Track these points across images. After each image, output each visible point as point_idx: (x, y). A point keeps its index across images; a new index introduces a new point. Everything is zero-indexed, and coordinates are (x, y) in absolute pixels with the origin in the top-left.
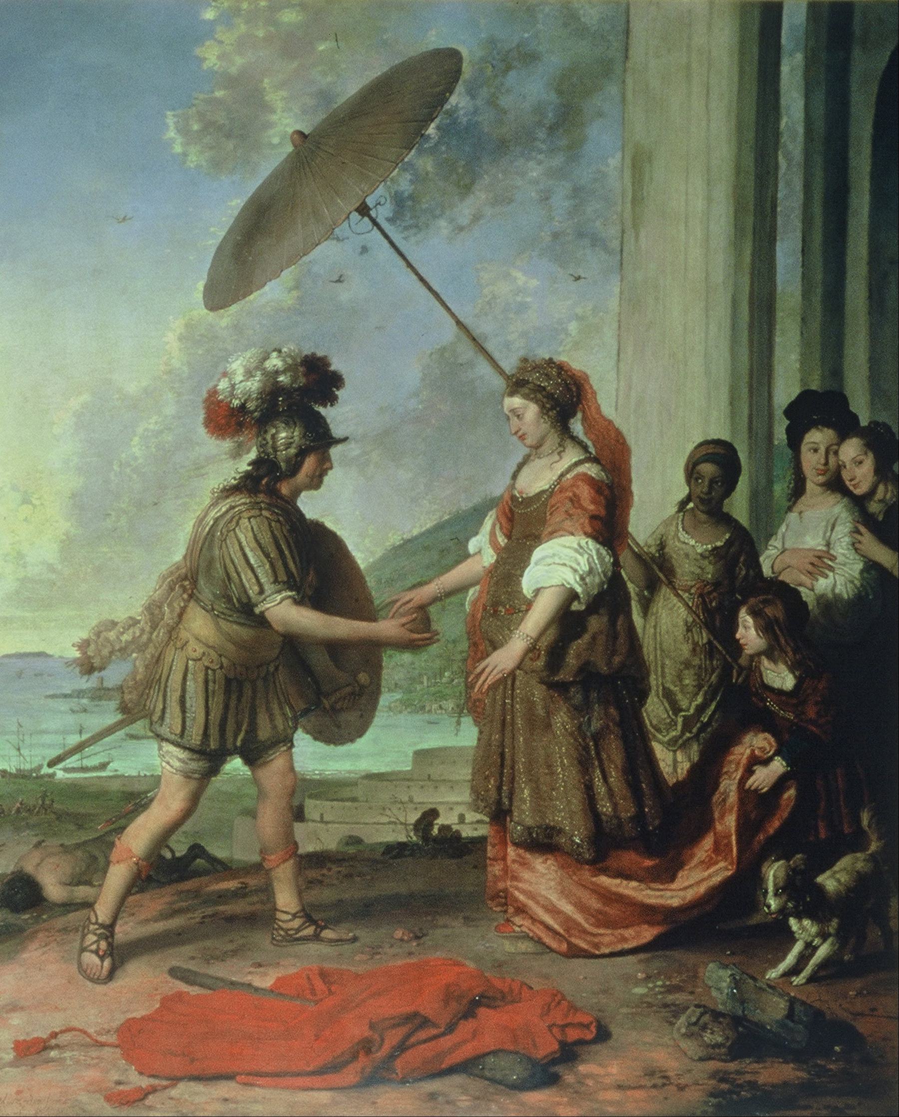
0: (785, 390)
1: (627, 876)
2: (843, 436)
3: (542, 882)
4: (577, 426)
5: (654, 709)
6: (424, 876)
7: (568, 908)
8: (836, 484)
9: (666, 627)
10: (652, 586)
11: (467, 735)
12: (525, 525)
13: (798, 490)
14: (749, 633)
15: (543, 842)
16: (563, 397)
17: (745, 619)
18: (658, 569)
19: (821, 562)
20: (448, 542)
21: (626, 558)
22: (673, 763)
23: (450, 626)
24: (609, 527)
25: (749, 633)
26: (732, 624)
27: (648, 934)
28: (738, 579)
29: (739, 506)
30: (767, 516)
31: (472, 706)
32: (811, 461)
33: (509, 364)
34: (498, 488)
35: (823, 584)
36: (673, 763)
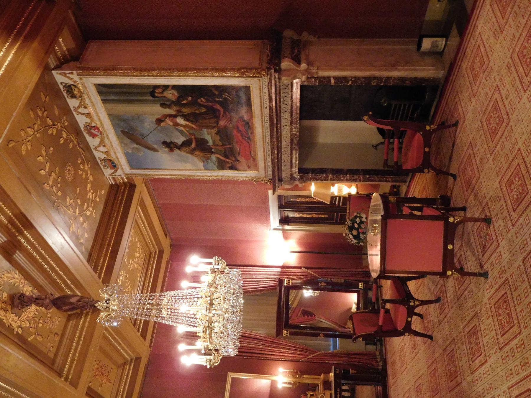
0: (151, 98)
1: (220, 115)
2: (155, 92)
3: (222, 123)
4: (163, 119)
5: (197, 112)
6: (224, 135)
7: (225, 121)
8: (162, 93)
9: (186, 110)
10: (181, 112)
11: (205, 130)
12: (176, 124)
13: (164, 97)
14: (185, 102)
15: (217, 123)
16: (159, 121)
17: (183, 102)
18: (178, 111)
19: (173, 94)
20: (181, 132)
21: (178, 114)
22: (204, 110)
23: (191, 132)
24: (175, 116)
25: (185, 102)
26: (184, 104)
27: (227, 113)
28: (177, 103)
29: (168, 103)
30: (169, 100)
31: (201, 129)
32: (160, 95)
33: (157, 126)
34: (173, 127)
35: (176, 94)
36: (204, 110)
